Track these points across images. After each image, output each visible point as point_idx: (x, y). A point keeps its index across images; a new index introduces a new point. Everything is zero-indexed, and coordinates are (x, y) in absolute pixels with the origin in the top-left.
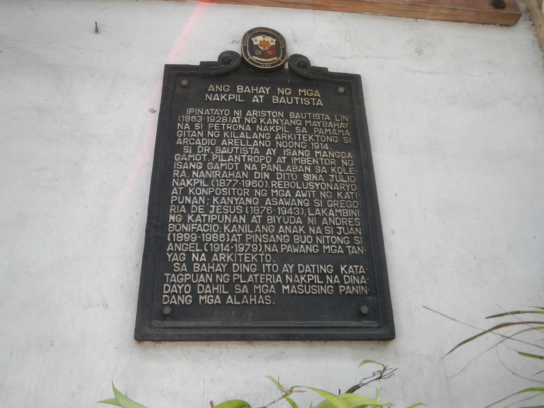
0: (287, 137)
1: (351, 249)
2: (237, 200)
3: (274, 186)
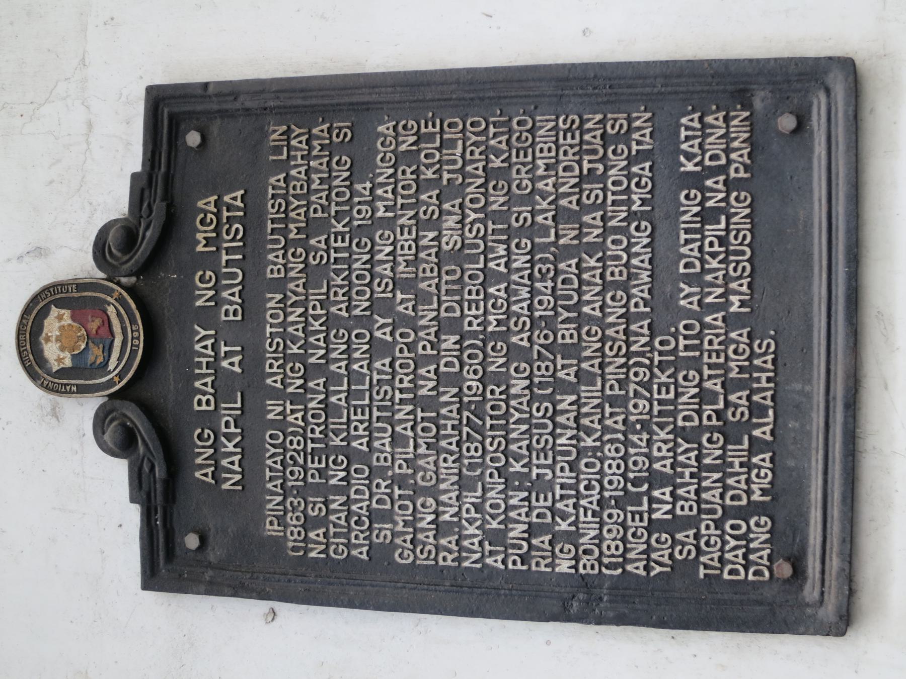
0: (341, 287)
1: (639, 143)
2: (517, 415)
3: (478, 325)
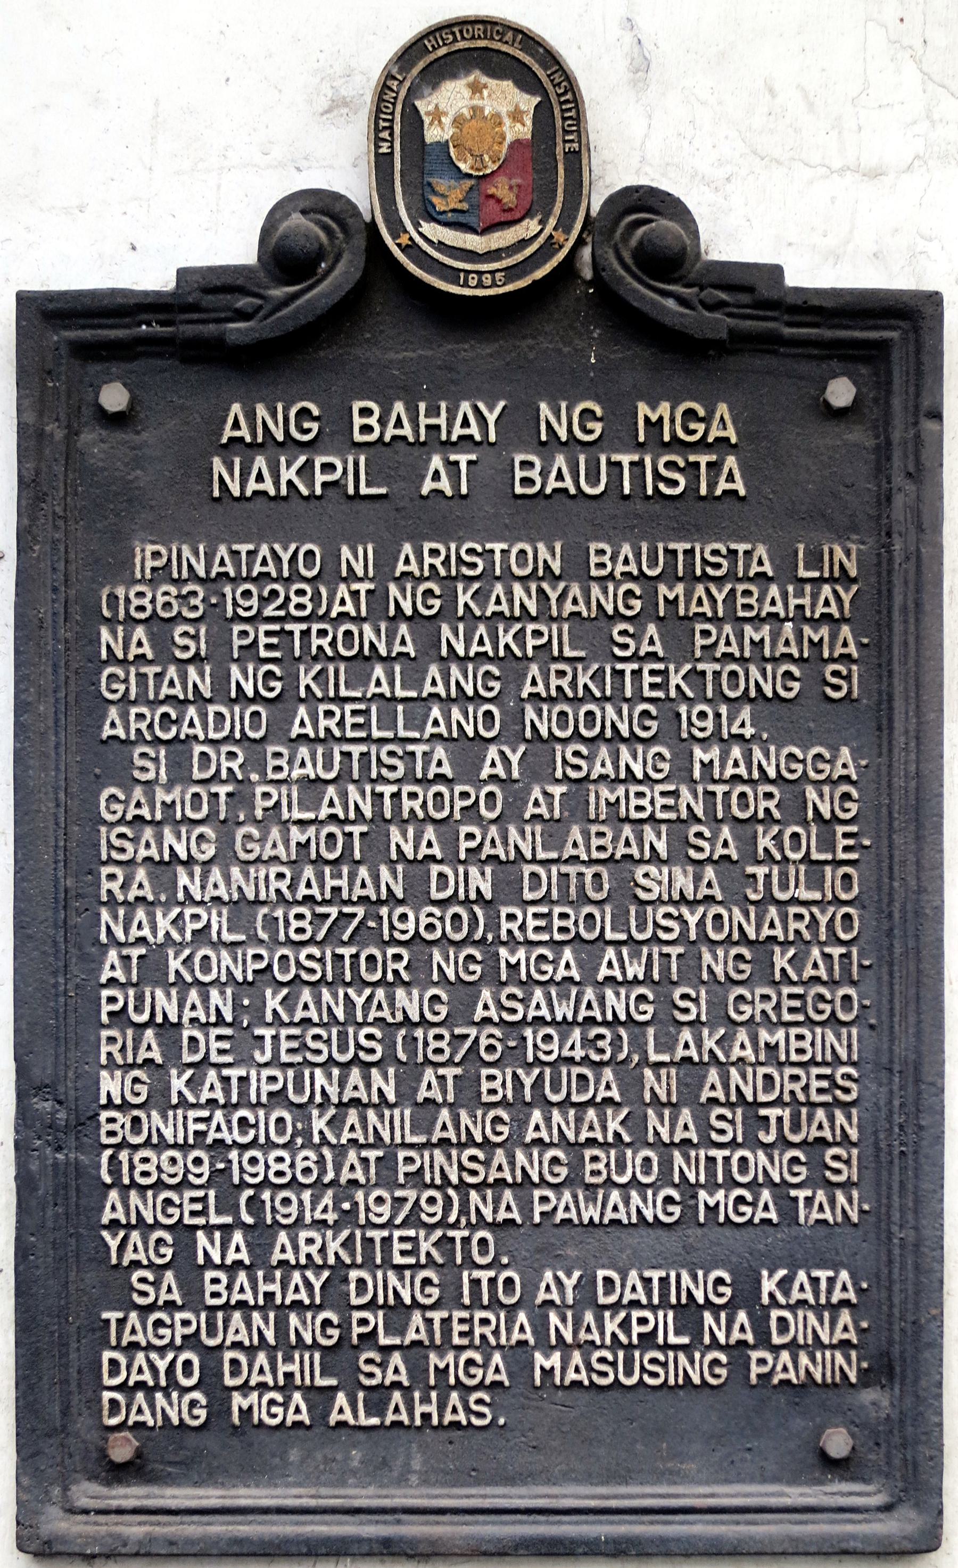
1: (809, 1201)
2: (360, 1001)
3: (509, 932)
